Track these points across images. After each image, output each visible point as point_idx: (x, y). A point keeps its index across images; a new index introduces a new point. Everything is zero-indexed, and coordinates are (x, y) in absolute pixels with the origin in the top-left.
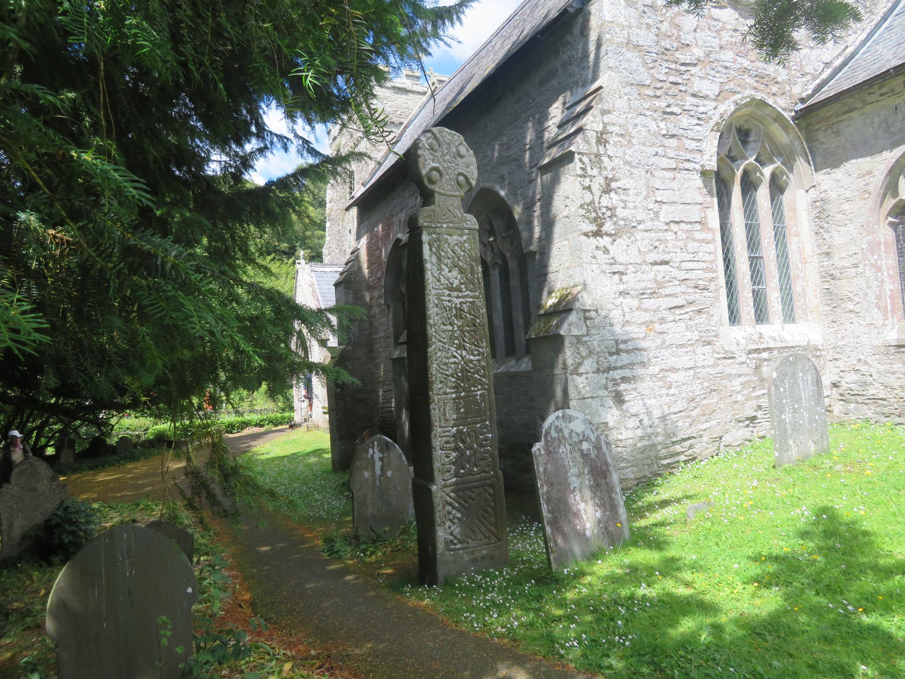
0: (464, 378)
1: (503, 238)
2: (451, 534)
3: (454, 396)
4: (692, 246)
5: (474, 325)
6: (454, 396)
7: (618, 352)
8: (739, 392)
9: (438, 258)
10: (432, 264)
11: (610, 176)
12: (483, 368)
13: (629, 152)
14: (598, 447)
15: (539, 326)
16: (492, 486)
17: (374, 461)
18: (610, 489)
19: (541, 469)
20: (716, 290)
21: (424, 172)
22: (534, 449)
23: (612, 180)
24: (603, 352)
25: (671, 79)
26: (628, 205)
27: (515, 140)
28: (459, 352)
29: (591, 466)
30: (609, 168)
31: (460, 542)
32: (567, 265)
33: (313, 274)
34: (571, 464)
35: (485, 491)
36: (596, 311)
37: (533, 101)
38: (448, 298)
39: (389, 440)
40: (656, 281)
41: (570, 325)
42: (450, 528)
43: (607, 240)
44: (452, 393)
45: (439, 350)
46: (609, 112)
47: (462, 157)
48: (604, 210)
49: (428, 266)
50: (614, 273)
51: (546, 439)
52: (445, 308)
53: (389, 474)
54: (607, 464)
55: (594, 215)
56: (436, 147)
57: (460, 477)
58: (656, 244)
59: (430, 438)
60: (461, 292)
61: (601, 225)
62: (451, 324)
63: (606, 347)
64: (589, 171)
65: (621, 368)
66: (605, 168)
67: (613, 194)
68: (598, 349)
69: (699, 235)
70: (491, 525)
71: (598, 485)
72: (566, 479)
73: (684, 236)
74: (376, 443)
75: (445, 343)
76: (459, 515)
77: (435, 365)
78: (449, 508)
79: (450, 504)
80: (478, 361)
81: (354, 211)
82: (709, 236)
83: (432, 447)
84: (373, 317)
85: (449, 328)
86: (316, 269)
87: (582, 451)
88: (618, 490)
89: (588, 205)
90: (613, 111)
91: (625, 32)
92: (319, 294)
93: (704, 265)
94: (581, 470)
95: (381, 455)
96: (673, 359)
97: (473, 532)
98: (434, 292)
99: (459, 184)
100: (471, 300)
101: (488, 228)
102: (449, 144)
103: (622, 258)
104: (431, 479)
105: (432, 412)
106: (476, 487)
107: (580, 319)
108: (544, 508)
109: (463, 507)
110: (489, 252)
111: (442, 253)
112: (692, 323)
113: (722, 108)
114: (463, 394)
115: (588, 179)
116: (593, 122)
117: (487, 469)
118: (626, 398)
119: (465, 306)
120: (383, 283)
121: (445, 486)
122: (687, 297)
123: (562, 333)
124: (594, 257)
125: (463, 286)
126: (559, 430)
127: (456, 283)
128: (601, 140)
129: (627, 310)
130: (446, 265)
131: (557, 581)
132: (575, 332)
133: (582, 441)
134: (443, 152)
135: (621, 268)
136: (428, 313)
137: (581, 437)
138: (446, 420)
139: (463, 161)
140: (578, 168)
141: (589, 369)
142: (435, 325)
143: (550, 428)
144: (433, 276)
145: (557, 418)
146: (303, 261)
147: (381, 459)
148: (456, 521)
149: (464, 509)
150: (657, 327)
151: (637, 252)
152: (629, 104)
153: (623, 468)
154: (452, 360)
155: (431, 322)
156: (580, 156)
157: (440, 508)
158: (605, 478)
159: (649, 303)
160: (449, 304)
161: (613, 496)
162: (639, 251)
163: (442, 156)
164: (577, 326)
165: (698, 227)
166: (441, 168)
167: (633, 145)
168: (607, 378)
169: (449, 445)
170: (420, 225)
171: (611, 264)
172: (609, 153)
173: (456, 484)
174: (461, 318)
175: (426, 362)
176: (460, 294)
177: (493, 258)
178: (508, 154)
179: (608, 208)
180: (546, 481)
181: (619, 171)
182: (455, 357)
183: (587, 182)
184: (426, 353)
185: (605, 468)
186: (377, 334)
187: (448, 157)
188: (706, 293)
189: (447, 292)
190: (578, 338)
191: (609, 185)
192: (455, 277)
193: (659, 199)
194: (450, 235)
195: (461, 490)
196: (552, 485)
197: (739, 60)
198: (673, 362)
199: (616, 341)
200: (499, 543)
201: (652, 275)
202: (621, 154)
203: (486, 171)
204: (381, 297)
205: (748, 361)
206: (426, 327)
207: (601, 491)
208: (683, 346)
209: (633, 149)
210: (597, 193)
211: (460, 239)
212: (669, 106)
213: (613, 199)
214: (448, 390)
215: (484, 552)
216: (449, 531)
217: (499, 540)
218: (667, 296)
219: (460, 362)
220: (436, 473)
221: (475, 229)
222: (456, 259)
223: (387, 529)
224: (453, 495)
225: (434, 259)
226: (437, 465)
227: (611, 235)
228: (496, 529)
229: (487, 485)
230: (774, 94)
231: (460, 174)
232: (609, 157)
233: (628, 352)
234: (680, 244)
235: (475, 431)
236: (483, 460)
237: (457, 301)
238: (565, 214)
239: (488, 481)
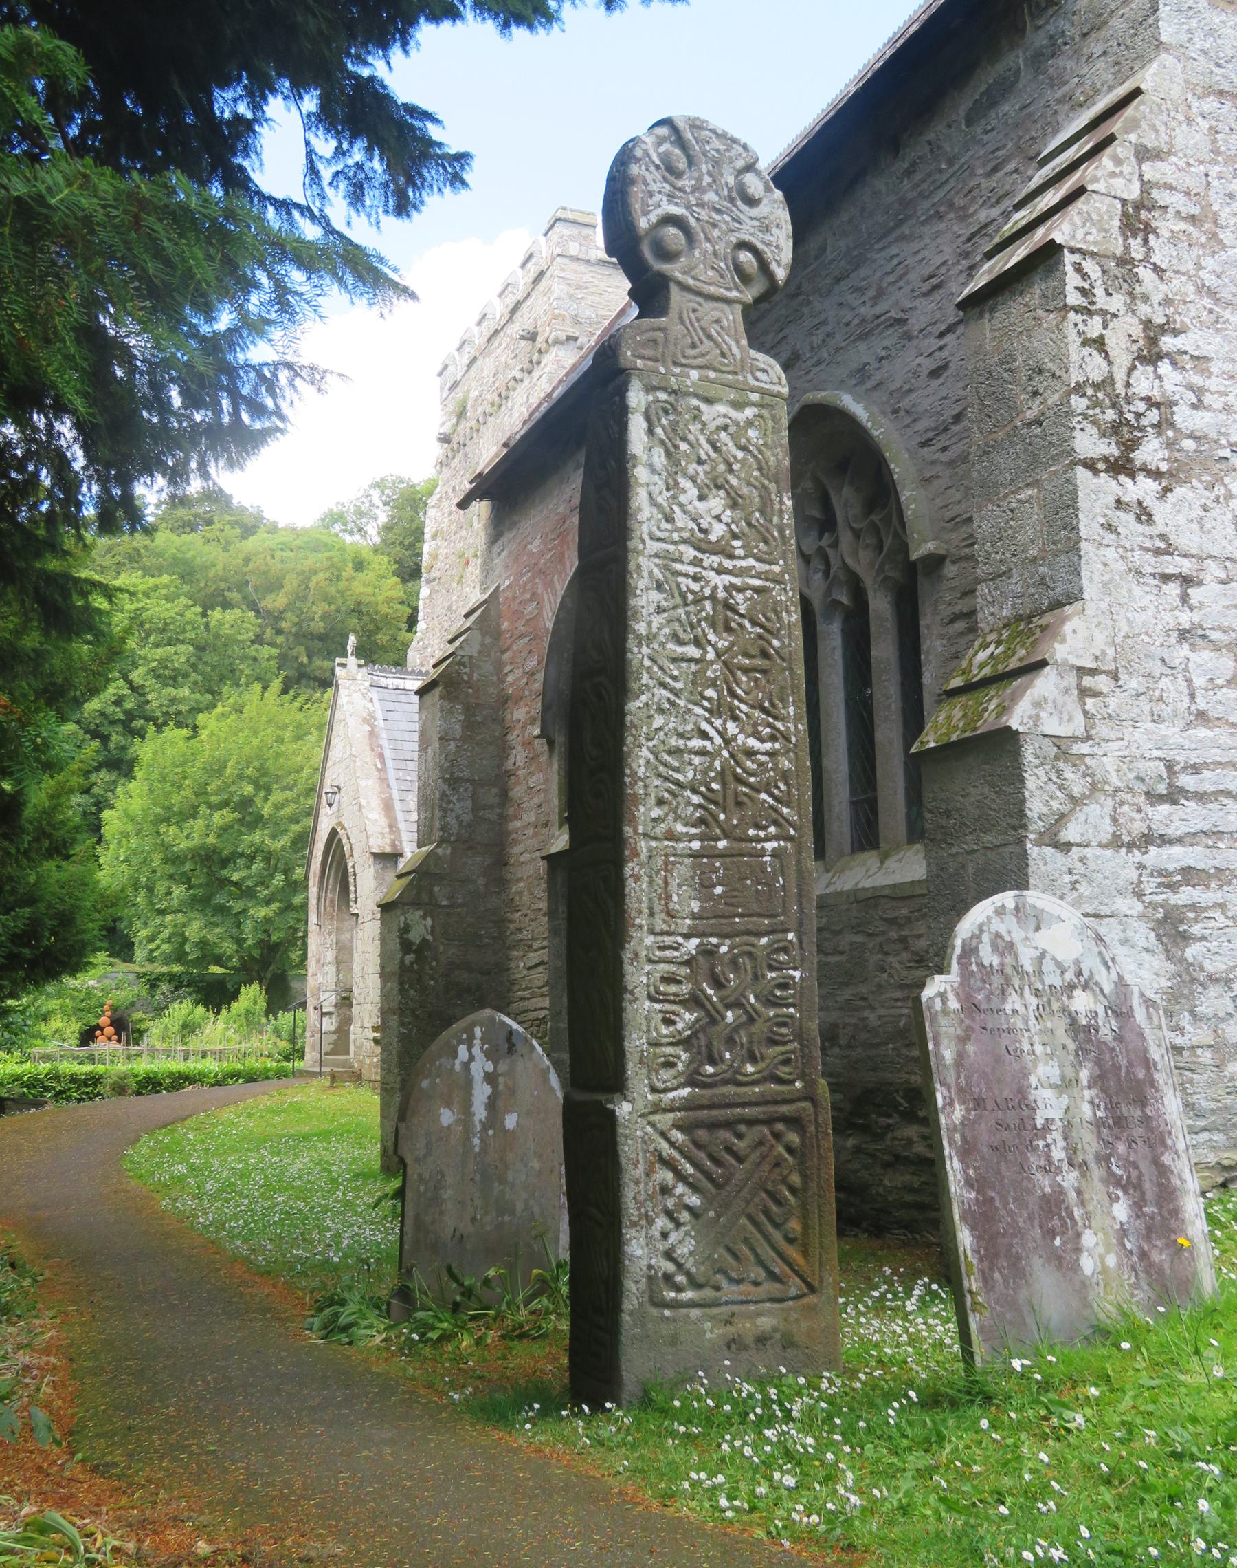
1: (857, 534)
2: (669, 1255)
3: (696, 845)
5: (765, 654)
6: (696, 845)
7: (1174, 796)
9: (668, 454)
10: (653, 471)
11: (1159, 319)
12: (785, 776)
13: (1209, 263)
14: (1121, 1012)
15: (949, 718)
16: (794, 1122)
17: (469, 1082)
19: (948, 1055)
21: (643, 223)
22: (928, 993)
23: (1163, 329)
24: (1130, 790)
26: (1208, 399)
27: (900, 271)
28: (718, 722)
29: (1098, 1062)
30: (1156, 298)
31: (695, 1284)
32: (1033, 551)
33: (374, 693)
34: (1039, 1049)
35: (777, 1136)
36: (1115, 676)
37: (951, 163)
38: (692, 570)
39: (515, 1026)
41: (1037, 705)
42: (665, 1235)
43: (1144, 488)
44: (692, 838)
45: (661, 711)
47: (752, 202)
48: (1141, 406)
49: (641, 473)
50: (1166, 578)
51: (964, 967)
52: (683, 596)
53: (511, 1121)
54: (1148, 1064)
55: (1110, 415)
56: (682, 165)
57: (704, 1086)
59: (620, 962)
60: (731, 557)
61: (1131, 445)
62: (697, 643)
63: (1140, 779)
64: (1101, 301)
65: (1179, 841)
66: (1146, 298)
67: (1164, 367)
68: (1115, 781)
70: (790, 1241)
71: (1120, 1122)
72: (1022, 1092)
74: (478, 1031)
75: (677, 694)
76: (694, 1200)
77: (645, 752)
78: (669, 1176)
79: (669, 1164)
80: (771, 754)
81: (481, 509)
83: (625, 989)
84: (510, 774)
85: (692, 651)
86: (384, 682)
87: (1073, 1022)
88: (1181, 1146)
89: (1097, 386)
90: (1170, 153)
92: (385, 743)
94: (1070, 1072)
95: (490, 1067)
97: (735, 1256)
98: (653, 547)
99: (738, 269)
100: (757, 583)
101: (816, 513)
102: (717, 163)
103: (1187, 539)
104: (617, 1084)
105: (630, 884)
106: (751, 1122)
107: (1067, 691)
108: (954, 1169)
109: (708, 1176)
110: (819, 576)
111: (683, 446)
114: (722, 844)
115: (1097, 320)
116: (1113, 175)
117: (783, 1071)
118: (1196, 930)
119: (740, 597)
120: (538, 686)
121: (657, 1108)
123: (1014, 724)
124: (1109, 527)
125: (737, 543)
126: (1005, 947)
127: (718, 531)
128: (1136, 219)
129: (1200, 681)
130: (693, 479)
131: (988, 1399)
132: (1051, 726)
133: (1071, 987)
134: (699, 180)
135: (1186, 566)
136: (632, 602)
137: (1070, 976)
138: (670, 914)
139: (755, 212)
140: (1069, 289)
141: (1090, 835)
142: (651, 638)
143: (977, 937)
144: (653, 503)
145: (1001, 911)
146: (352, 661)
148: (685, 1216)
149: (713, 1184)
152: (1214, 141)
154: (696, 743)
155: (641, 628)
156: (1077, 258)
157: (639, 1172)
158: (1143, 1102)
160: (695, 587)
161: (1166, 1159)
163: (695, 189)
164: (1058, 709)
166: (692, 222)
167: (1223, 247)
168: (1141, 866)
169: (673, 988)
170: (623, 363)
171: (1158, 552)
172: (1156, 259)
173: (689, 1105)
174: (729, 629)
175: (620, 741)
176: (728, 564)
177: (828, 592)
178: (878, 310)
180: (961, 1090)
181: (1182, 308)
182: (704, 735)
183: (1094, 327)
184: (621, 714)
185: (1141, 1074)
186: (517, 817)
187: (710, 196)
189: (690, 553)
190: (1062, 747)
191: (1153, 341)
194: (709, 401)
195: (705, 1123)
196: (979, 1103)
199: (1170, 765)
200: (811, 1299)
202: (1190, 266)
203: (819, 363)
204: (533, 721)
206: (624, 640)
207: (1131, 1142)
209: (1223, 255)
210: (1122, 360)
211: (734, 414)
213: (1170, 379)
214: (680, 828)
215: (766, 1323)
216: (662, 1246)
217: (812, 1289)
219: (717, 753)
220: (632, 1067)
221: (778, 395)
222: (722, 467)
223: (492, 1273)
224: (678, 1136)
225: (659, 458)
226: (635, 1042)
227: (1156, 475)
228: (805, 1253)
229: (785, 1119)
231: (743, 245)
232: (1157, 269)
233: (1201, 797)
235: (750, 954)
236: (772, 1042)
237: (720, 581)
238: (1030, 415)
239: (785, 1109)
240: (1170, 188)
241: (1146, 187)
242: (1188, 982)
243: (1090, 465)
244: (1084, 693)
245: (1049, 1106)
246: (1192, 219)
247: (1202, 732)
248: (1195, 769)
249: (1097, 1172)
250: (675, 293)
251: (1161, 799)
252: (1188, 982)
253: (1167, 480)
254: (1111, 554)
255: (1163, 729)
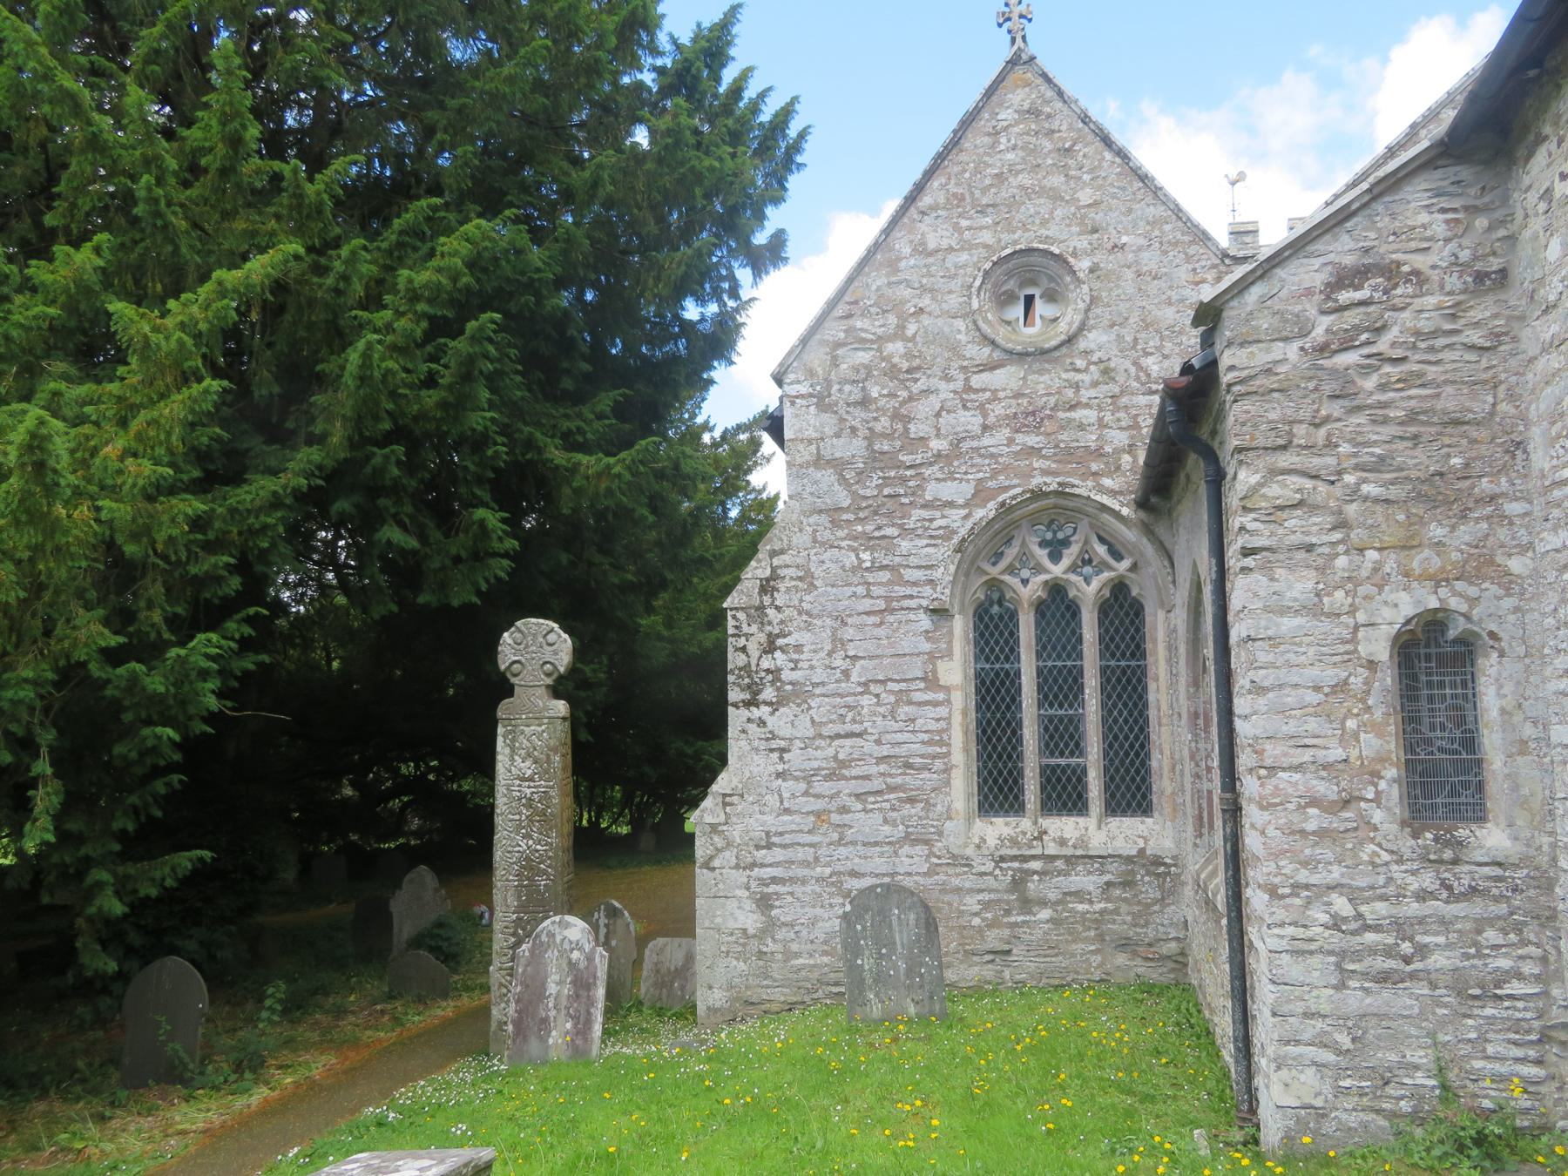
0: (529, 866)
4: (904, 711)
7: (769, 846)
8: (976, 914)
13: (807, 598)
18: (591, 1002)
20: (945, 771)
21: (503, 667)
23: (778, 636)
25: (886, 491)
36: (742, 796)
40: (835, 757)
46: (782, 552)
49: (499, 757)
50: (772, 750)
54: (595, 977)
55: (747, 680)
58: (843, 711)
62: (520, 813)
64: (745, 629)
65: (771, 865)
66: (770, 623)
67: (778, 654)
69: (919, 697)
73: (892, 699)
82: (941, 696)
89: (740, 669)
91: (813, 447)
93: (926, 737)
96: (857, 860)
112: (895, 814)
113: (979, 513)
122: (889, 780)
124: (744, 731)
126: (551, 935)
127: (529, 772)
128: (767, 587)
129: (786, 795)
132: (709, 819)
135: (783, 744)
147: (606, 926)
150: (835, 818)
151: (809, 724)
153: (768, 987)
155: (498, 811)
159: (820, 787)
162: (813, 721)
165: (922, 685)
167: (816, 588)
171: (767, 739)
179: (768, 671)
188: (926, 775)
190: (714, 828)
192: (528, 768)
193: (851, 653)
197: (1020, 438)
198: (857, 863)
201: (831, 751)
205: (997, 872)
208: (876, 844)
212: (879, 528)
218: (855, 778)
225: (507, 750)
226: (496, 947)
230: (1095, 474)
232: (778, 608)
233: (784, 846)
234: (882, 710)
237: (528, 791)
240: (788, 566)
241: (774, 570)
242: (770, 927)
243: (735, 705)
244: (725, 804)
245: (552, 988)
246: (800, 579)
247: (786, 818)
248: (781, 834)
249: (563, 1012)
250: (517, 690)
251: (763, 848)
252: (770, 927)
253: (775, 706)
254: (743, 743)
255: (765, 817)
